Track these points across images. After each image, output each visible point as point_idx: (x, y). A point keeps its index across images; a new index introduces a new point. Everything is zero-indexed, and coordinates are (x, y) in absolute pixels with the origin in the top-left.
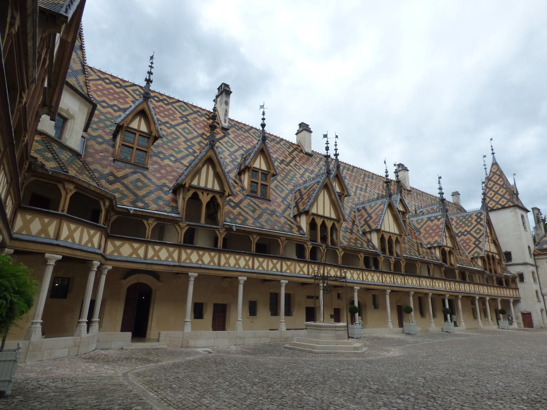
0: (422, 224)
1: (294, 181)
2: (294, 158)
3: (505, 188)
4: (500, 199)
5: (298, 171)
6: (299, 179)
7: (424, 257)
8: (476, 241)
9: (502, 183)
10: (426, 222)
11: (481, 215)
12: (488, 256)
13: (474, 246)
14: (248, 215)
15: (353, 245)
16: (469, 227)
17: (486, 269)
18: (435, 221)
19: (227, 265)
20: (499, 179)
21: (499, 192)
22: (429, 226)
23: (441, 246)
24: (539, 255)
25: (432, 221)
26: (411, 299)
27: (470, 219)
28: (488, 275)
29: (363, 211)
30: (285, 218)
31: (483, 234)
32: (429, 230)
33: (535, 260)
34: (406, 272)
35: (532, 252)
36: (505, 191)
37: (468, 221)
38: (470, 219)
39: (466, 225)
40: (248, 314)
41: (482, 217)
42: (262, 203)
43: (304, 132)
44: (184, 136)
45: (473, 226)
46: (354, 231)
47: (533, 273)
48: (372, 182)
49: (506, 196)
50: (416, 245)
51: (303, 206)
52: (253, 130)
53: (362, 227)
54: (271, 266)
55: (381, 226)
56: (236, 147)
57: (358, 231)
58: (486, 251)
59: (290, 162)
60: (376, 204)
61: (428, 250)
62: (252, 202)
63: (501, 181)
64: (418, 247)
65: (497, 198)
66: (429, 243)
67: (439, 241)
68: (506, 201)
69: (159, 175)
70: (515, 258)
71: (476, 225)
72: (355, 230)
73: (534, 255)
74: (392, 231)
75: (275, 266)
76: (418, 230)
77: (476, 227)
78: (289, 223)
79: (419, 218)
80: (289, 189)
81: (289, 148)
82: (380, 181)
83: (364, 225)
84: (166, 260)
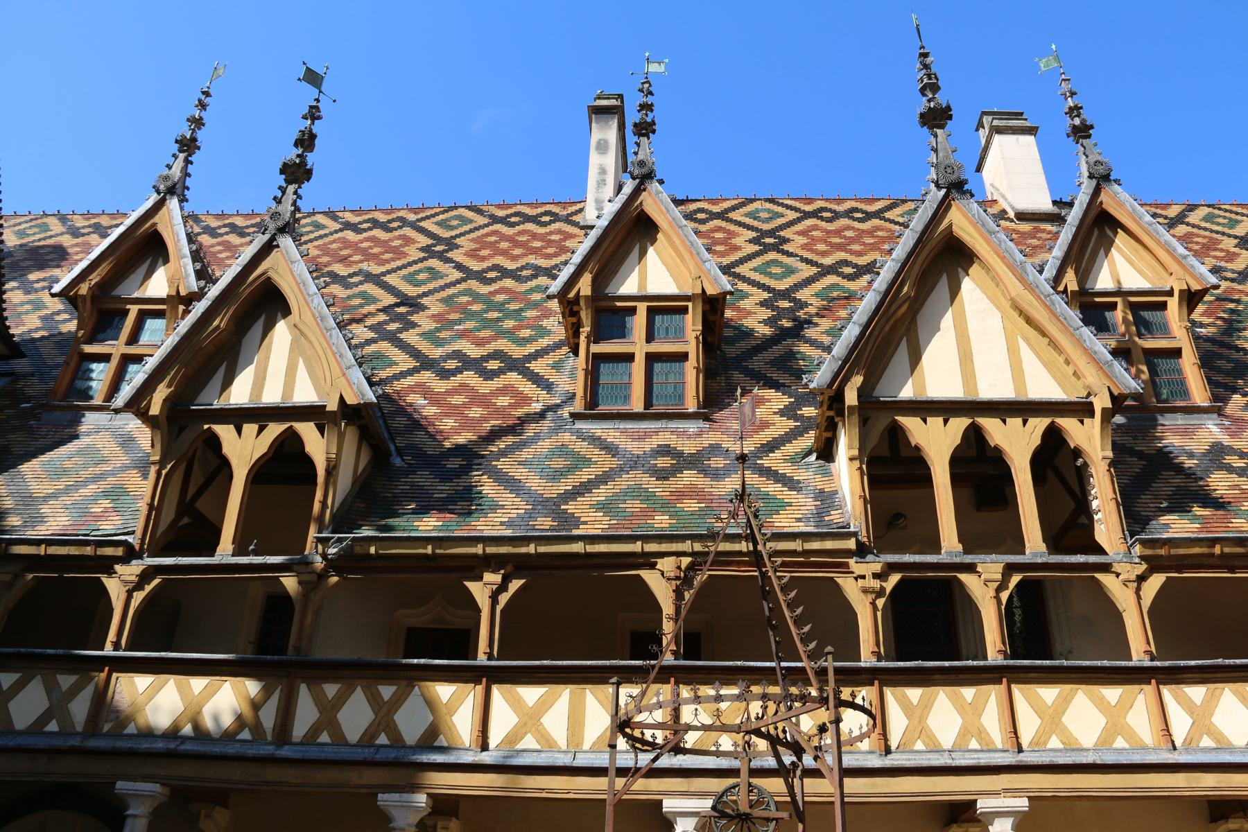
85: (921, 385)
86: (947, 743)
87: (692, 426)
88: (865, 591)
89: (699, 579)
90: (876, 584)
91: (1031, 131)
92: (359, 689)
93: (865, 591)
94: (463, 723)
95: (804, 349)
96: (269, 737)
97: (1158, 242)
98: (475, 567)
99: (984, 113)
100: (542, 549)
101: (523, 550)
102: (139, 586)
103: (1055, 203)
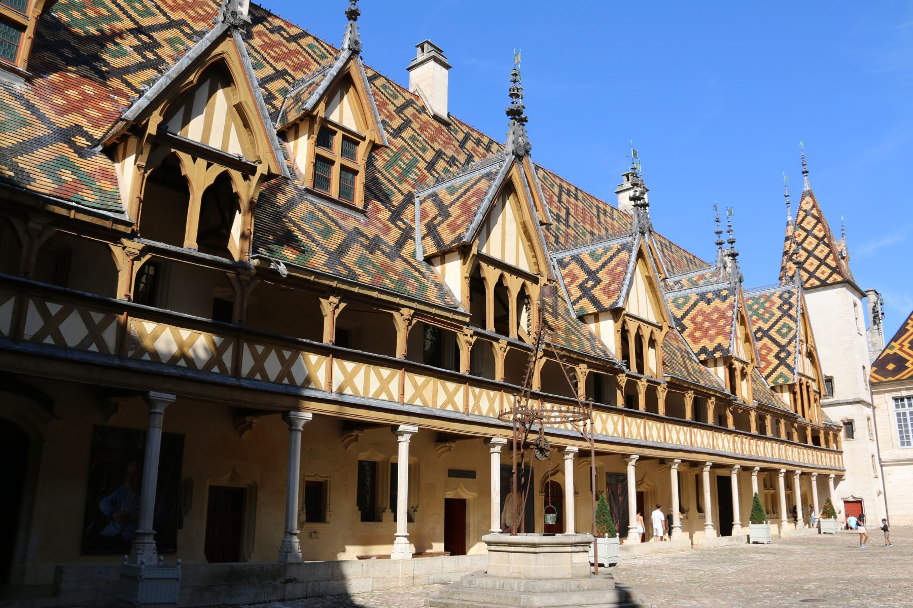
0: (686, 308)
1: (413, 176)
2: (407, 123)
3: (828, 245)
5: (420, 152)
6: (425, 172)
7: (698, 381)
8: (780, 352)
9: (821, 235)
10: (695, 305)
11: (790, 297)
12: (801, 385)
13: (777, 362)
14: (313, 240)
15: (563, 343)
16: (766, 321)
17: (796, 412)
18: (717, 303)
19: (258, 377)
20: (816, 225)
22: (702, 312)
23: (731, 357)
25: (709, 302)
26: (674, 474)
27: (767, 305)
29: (574, 266)
30: (405, 260)
31: (795, 337)
32: (703, 321)
33: (872, 394)
34: (667, 413)
35: (868, 378)
36: (827, 250)
37: (764, 308)
38: (767, 305)
39: (761, 317)
40: (304, 518)
42: (344, 218)
43: (432, 63)
44: (129, 16)
45: (774, 319)
46: (560, 312)
47: (869, 419)
48: (576, 206)
49: (829, 261)
50: (679, 354)
51: (453, 231)
52: (309, 40)
53: (574, 304)
54: (375, 385)
56: (269, 71)
57: (567, 310)
58: (799, 374)
59: (401, 129)
60: (607, 250)
61: (702, 367)
62: (320, 210)
63: (820, 231)
64: (683, 357)
65: (812, 264)
66: (704, 350)
67: (726, 346)
68: (828, 271)
69: (60, 101)
70: (841, 392)
72: (561, 311)
73: (872, 384)
74: (643, 316)
75: (384, 385)
76: (679, 321)
77: (781, 323)
78: (416, 274)
79: (679, 294)
80: (406, 192)
81: (395, 97)
82: (591, 207)
83: (580, 298)
84: (83, 347)
85: (488, 249)
86: (484, 414)
87: (362, 219)
88: (467, 342)
89: (414, 321)
90: (470, 339)
91: (447, 67)
92: (273, 351)
93: (467, 342)
94: (321, 376)
95: (379, 175)
96: (229, 372)
97: (538, 194)
98: (328, 292)
99: (427, 42)
100: (361, 291)
101: (353, 289)
102: (138, 258)
103: (449, 115)
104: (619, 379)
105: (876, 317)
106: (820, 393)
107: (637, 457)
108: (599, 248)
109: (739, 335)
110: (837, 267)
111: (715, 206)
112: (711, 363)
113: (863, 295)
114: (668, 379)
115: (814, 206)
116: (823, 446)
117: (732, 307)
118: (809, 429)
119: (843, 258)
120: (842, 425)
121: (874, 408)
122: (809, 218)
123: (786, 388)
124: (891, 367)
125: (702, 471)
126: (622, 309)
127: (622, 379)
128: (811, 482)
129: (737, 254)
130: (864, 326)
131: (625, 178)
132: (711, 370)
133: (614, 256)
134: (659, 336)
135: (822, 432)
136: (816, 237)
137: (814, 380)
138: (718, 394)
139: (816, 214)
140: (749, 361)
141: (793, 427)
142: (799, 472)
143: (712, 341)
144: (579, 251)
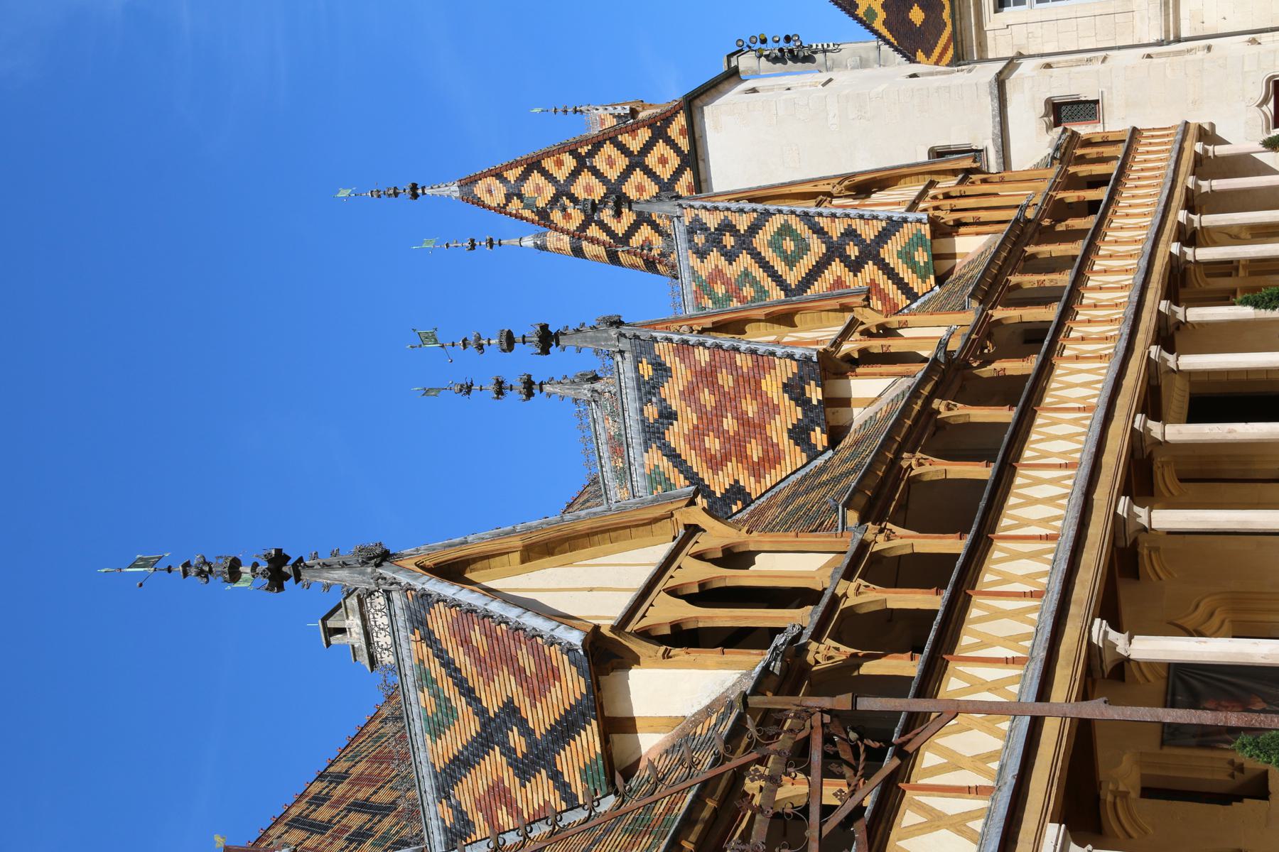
3: (597, 145)
4: (649, 172)
8: (845, 259)
10: (673, 456)
11: (704, 228)
13: (870, 269)
18: (672, 392)
21: (613, 175)
22: (696, 437)
23: (824, 355)
24: (958, 40)
25: (668, 416)
26: (1166, 519)
27: (720, 290)
28: (1042, 214)
31: (806, 217)
32: (720, 433)
33: (983, 59)
36: (608, 149)
38: (720, 290)
41: (712, 221)
45: (758, 273)
47: (1048, 66)
49: (635, 145)
50: (801, 500)
55: (564, 619)
60: (425, 680)
61: (848, 441)
63: (560, 164)
66: (799, 434)
67: (793, 367)
68: (661, 148)
71: (757, 256)
73: (959, 59)
77: (768, 254)
83: (556, 776)
104: (825, 664)
105: (793, 54)
106: (968, 172)
107: (1099, 628)
108: (420, 703)
109: (772, 338)
110: (651, 126)
111: (427, 392)
112: (839, 416)
113: (733, 75)
114: (853, 517)
115: (499, 176)
116: (1112, 168)
117: (684, 347)
118: (1061, 195)
119: (634, 113)
120: (1060, 129)
121: (1020, 56)
122: (528, 188)
123: (942, 245)
124: (917, 15)
125: (1162, 444)
126: (595, 638)
127: (826, 653)
128: (1213, 193)
129: (544, 328)
130: (810, 76)
131: (336, 639)
132: (859, 415)
133: (441, 654)
134: (717, 535)
135: (1072, 170)
136: (575, 174)
137: (932, 184)
138: (926, 391)
139: (520, 170)
140: (848, 317)
141: (1052, 227)
142: (1182, 216)
143: (776, 409)
144: (425, 770)
